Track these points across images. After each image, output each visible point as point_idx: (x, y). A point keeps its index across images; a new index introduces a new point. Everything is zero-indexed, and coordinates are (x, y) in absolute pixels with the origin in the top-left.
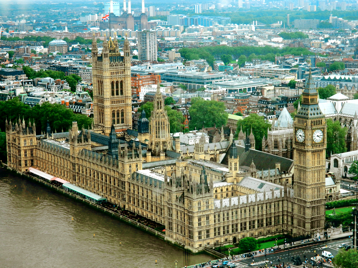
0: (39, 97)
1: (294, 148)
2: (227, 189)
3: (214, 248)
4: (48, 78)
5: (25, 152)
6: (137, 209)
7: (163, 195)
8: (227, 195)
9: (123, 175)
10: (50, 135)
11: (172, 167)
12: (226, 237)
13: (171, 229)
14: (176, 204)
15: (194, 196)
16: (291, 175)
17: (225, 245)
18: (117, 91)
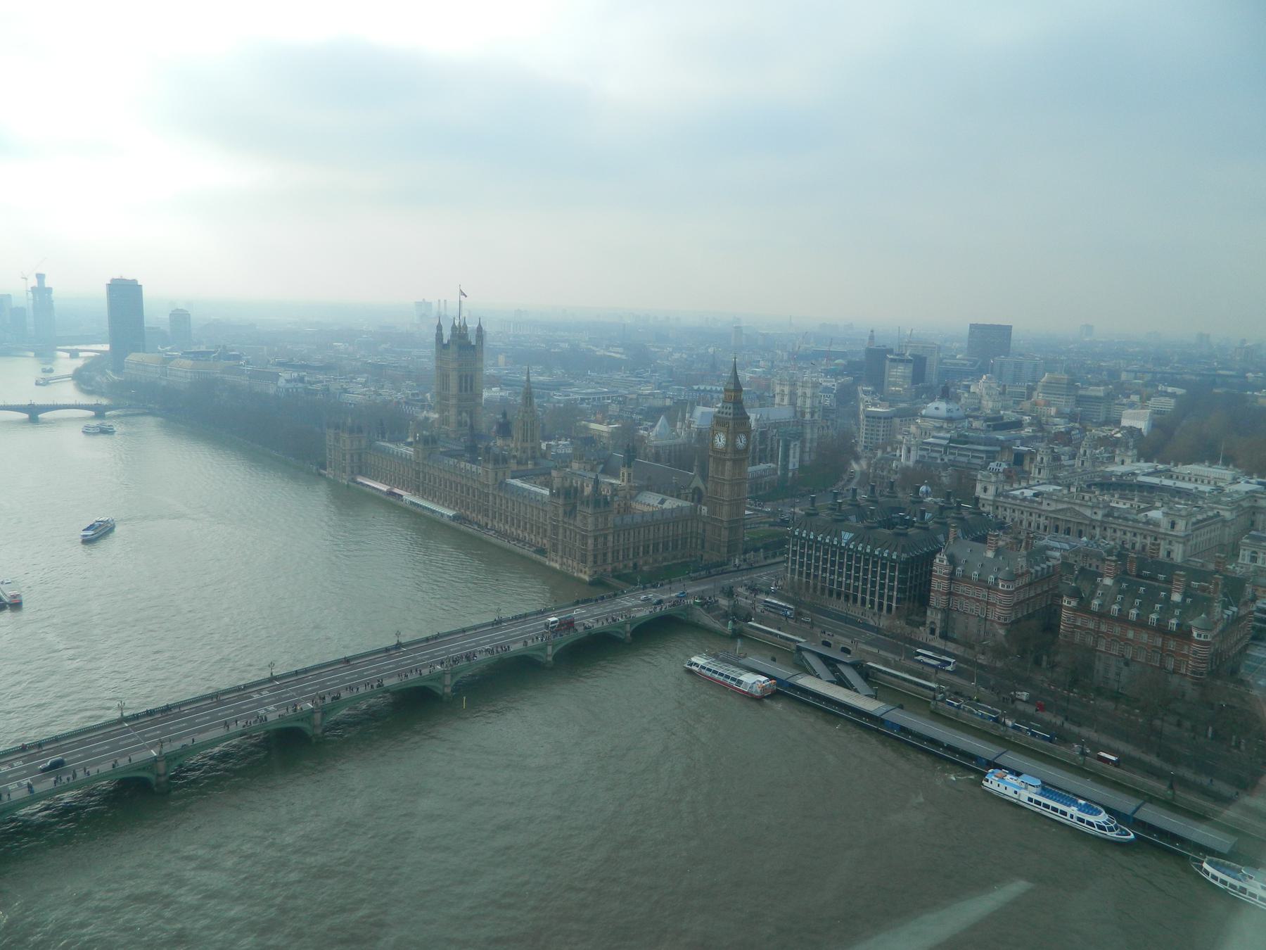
0: (358, 394)
1: (710, 456)
2: (619, 505)
3: (611, 575)
4: (366, 375)
5: (352, 456)
6: (504, 527)
7: (543, 510)
8: (619, 512)
9: (487, 486)
10: (383, 437)
11: (546, 476)
12: (625, 562)
13: (556, 551)
14: (565, 520)
15: (590, 510)
16: (691, 491)
17: (624, 572)
18: (466, 388)
